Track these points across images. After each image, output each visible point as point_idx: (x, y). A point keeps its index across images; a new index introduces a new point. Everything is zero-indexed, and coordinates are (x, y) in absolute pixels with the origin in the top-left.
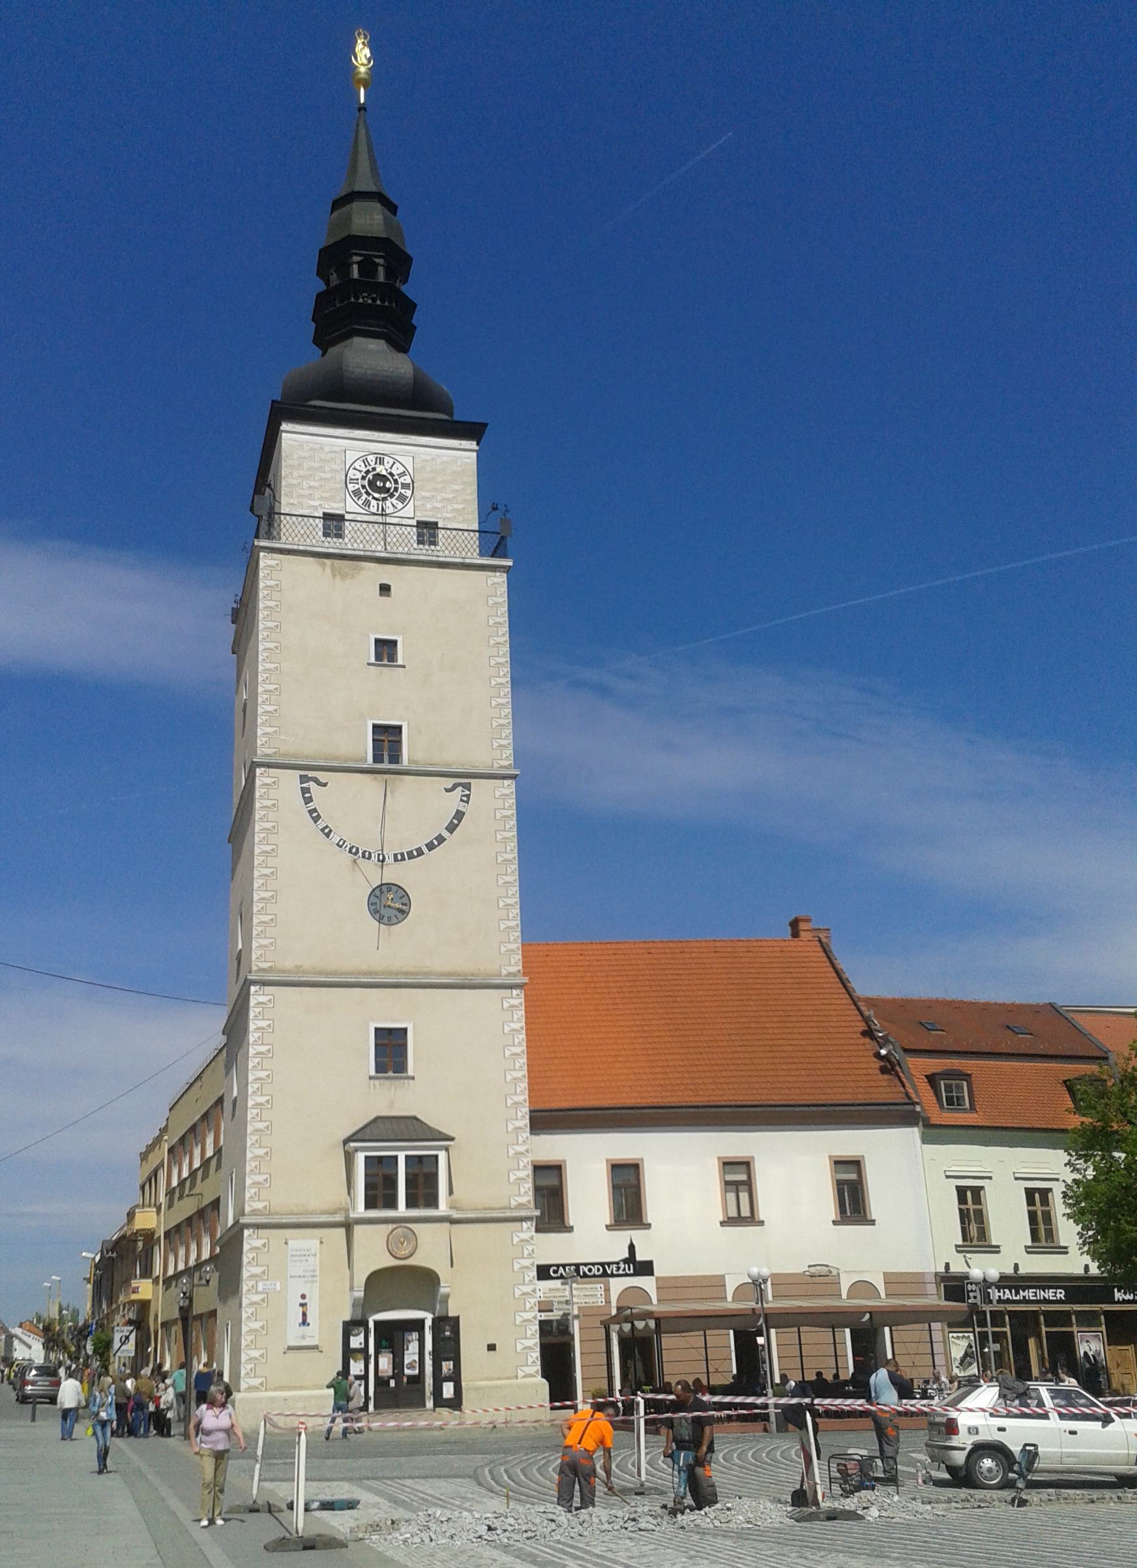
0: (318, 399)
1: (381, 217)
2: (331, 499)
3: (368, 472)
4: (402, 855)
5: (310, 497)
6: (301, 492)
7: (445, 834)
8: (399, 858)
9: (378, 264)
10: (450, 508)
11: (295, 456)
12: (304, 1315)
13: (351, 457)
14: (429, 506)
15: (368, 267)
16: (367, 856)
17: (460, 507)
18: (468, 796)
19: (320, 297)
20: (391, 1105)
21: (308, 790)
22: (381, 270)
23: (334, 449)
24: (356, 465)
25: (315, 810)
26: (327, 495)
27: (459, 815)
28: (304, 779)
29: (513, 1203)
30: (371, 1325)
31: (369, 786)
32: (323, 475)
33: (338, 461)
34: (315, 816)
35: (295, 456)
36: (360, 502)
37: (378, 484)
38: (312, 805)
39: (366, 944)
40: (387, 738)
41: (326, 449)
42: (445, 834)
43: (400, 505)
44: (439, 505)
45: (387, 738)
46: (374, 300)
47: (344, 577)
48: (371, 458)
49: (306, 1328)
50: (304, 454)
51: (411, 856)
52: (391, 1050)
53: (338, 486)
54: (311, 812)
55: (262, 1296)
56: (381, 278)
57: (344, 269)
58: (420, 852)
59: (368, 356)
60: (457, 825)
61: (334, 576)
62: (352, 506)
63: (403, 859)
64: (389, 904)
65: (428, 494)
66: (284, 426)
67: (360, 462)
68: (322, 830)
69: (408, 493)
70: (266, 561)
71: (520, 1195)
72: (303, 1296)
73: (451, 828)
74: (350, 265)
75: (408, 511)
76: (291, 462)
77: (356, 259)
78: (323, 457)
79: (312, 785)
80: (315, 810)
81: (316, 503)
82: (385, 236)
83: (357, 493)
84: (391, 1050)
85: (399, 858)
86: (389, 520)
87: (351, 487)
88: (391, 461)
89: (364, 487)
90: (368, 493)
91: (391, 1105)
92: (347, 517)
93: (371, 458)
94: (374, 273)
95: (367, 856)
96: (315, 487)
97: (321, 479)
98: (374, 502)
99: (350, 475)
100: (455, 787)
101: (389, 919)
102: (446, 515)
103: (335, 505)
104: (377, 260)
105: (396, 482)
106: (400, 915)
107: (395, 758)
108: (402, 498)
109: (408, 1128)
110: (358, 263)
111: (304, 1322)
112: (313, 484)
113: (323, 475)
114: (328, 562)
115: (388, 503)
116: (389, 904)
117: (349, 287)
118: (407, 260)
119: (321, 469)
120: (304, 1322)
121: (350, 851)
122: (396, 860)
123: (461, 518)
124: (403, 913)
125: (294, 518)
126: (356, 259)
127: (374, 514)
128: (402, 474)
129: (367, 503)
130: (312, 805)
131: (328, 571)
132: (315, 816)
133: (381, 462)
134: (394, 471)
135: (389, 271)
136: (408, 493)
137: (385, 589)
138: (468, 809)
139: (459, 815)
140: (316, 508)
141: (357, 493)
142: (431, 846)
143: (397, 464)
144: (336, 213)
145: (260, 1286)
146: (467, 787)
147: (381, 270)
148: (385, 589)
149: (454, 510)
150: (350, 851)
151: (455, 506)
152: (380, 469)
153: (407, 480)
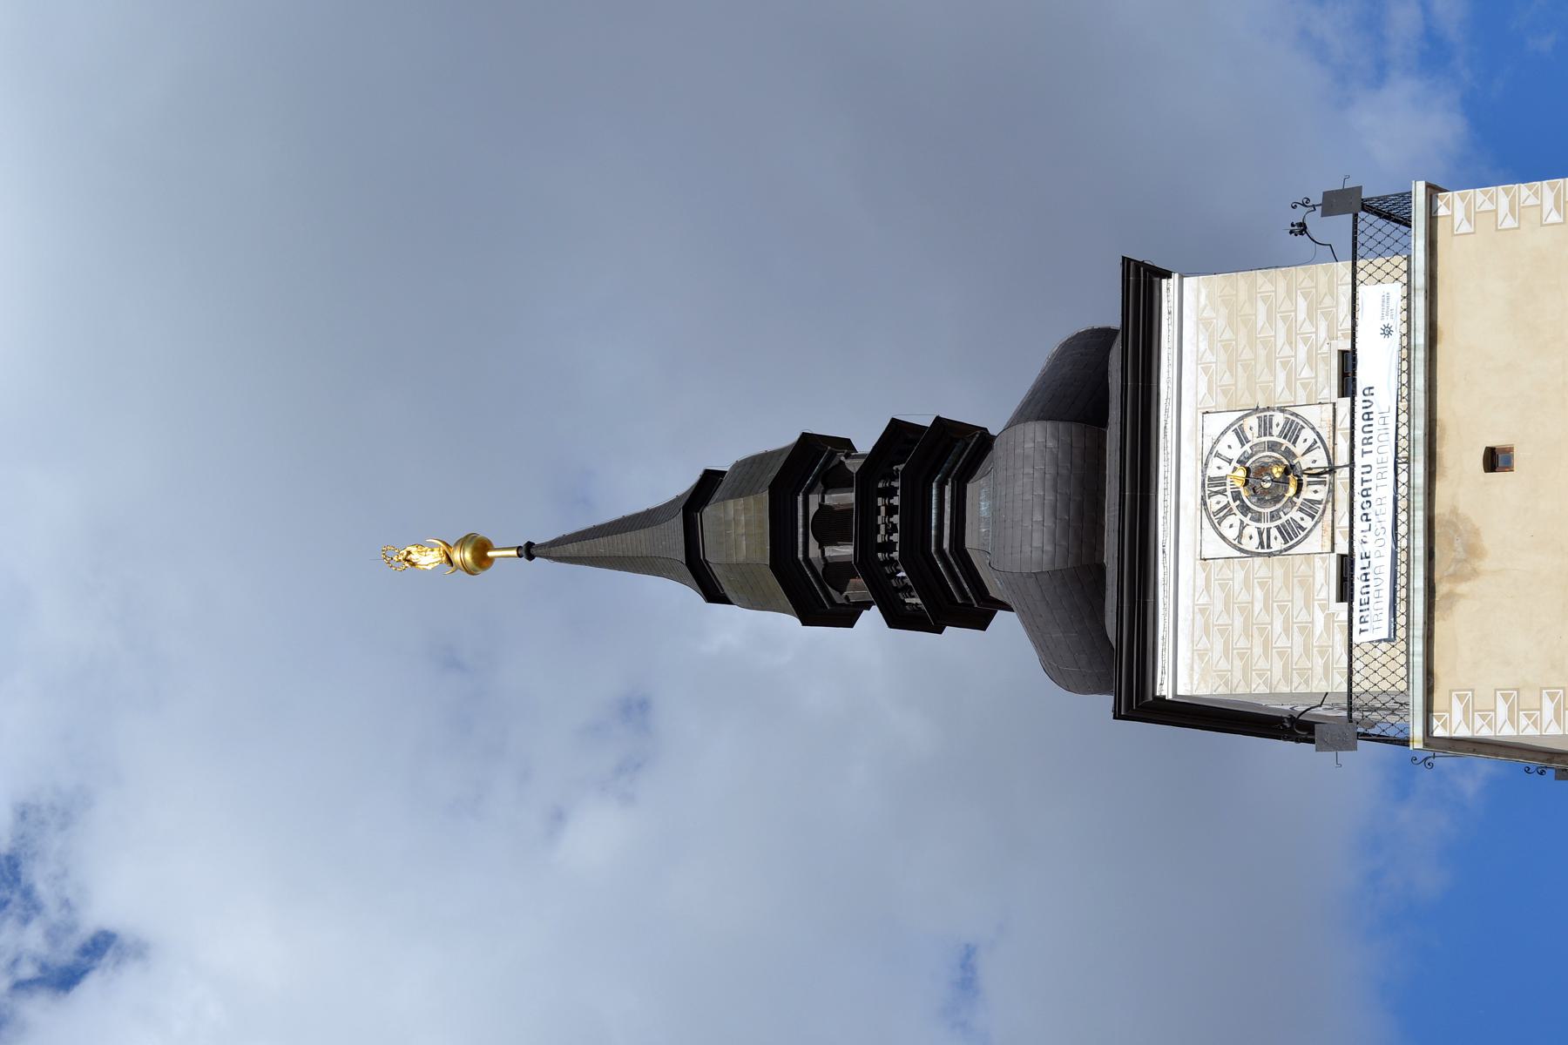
0: (1103, 627)
1: (731, 503)
2: (1307, 584)
3: (1245, 509)
6: (1298, 650)
9: (822, 506)
11: (1223, 665)
13: (1214, 547)
14: (1306, 373)
15: (829, 526)
17: (1302, 304)
19: (898, 618)
22: (832, 499)
23: (1201, 582)
24: (1231, 534)
26: (1299, 593)
32: (1258, 606)
33: (1227, 573)
35: (1223, 665)
36: (1308, 523)
37: (1271, 482)
41: (1203, 600)
43: (1308, 434)
44: (1302, 351)
46: (891, 510)
47: (1473, 551)
48: (1214, 503)
50: (1218, 646)
53: (1279, 572)
56: (848, 498)
57: (837, 573)
59: (1011, 518)
61: (1475, 573)
62: (1316, 542)
65: (1281, 377)
66: (1164, 690)
69: (1279, 418)
70: (1453, 723)
71: (1496, 211)
74: (828, 564)
75: (1318, 416)
76: (1238, 675)
77: (814, 551)
78: (1219, 606)
81: (1319, 617)
82: (766, 495)
83: (1288, 532)
86: (1342, 458)
87: (1277, 544)
88: (1215, 462)
92: (1343, 548)
93: (1214, 503)
94: (845, 513)
96: (1286, 620)
97: (1267, 607)
98: (1307, 493)
99: (1252, 545)
102: (1323, 334)
103: (1320, 576)
104: (813, 509)
108: (1291, 432)
110: (821, 547)
112: (1278, 627)
113: (1258, 606)
114: (1441, 589)
115: (1305, 462)
117: (868, 564)
118: (809, 445)
119: (1247, 611)
123: (1328, 301)
125: (1357, 665)
126: (814, 551)
127: (1332, 491)
129: (1310, 508)
131: (1462, 588)
133: (1221, 481)
134: (1236, 452)
135: (835, 479)
136: (1279, 418)
137: (1495, 460)
140: (1330, 617)
141: (1288, 532)
144: (730, 596)
147: (832, 499)
148: (1495, 460)
149: (1311, 315)
151: (1302, 315)
153: (1252, 421)
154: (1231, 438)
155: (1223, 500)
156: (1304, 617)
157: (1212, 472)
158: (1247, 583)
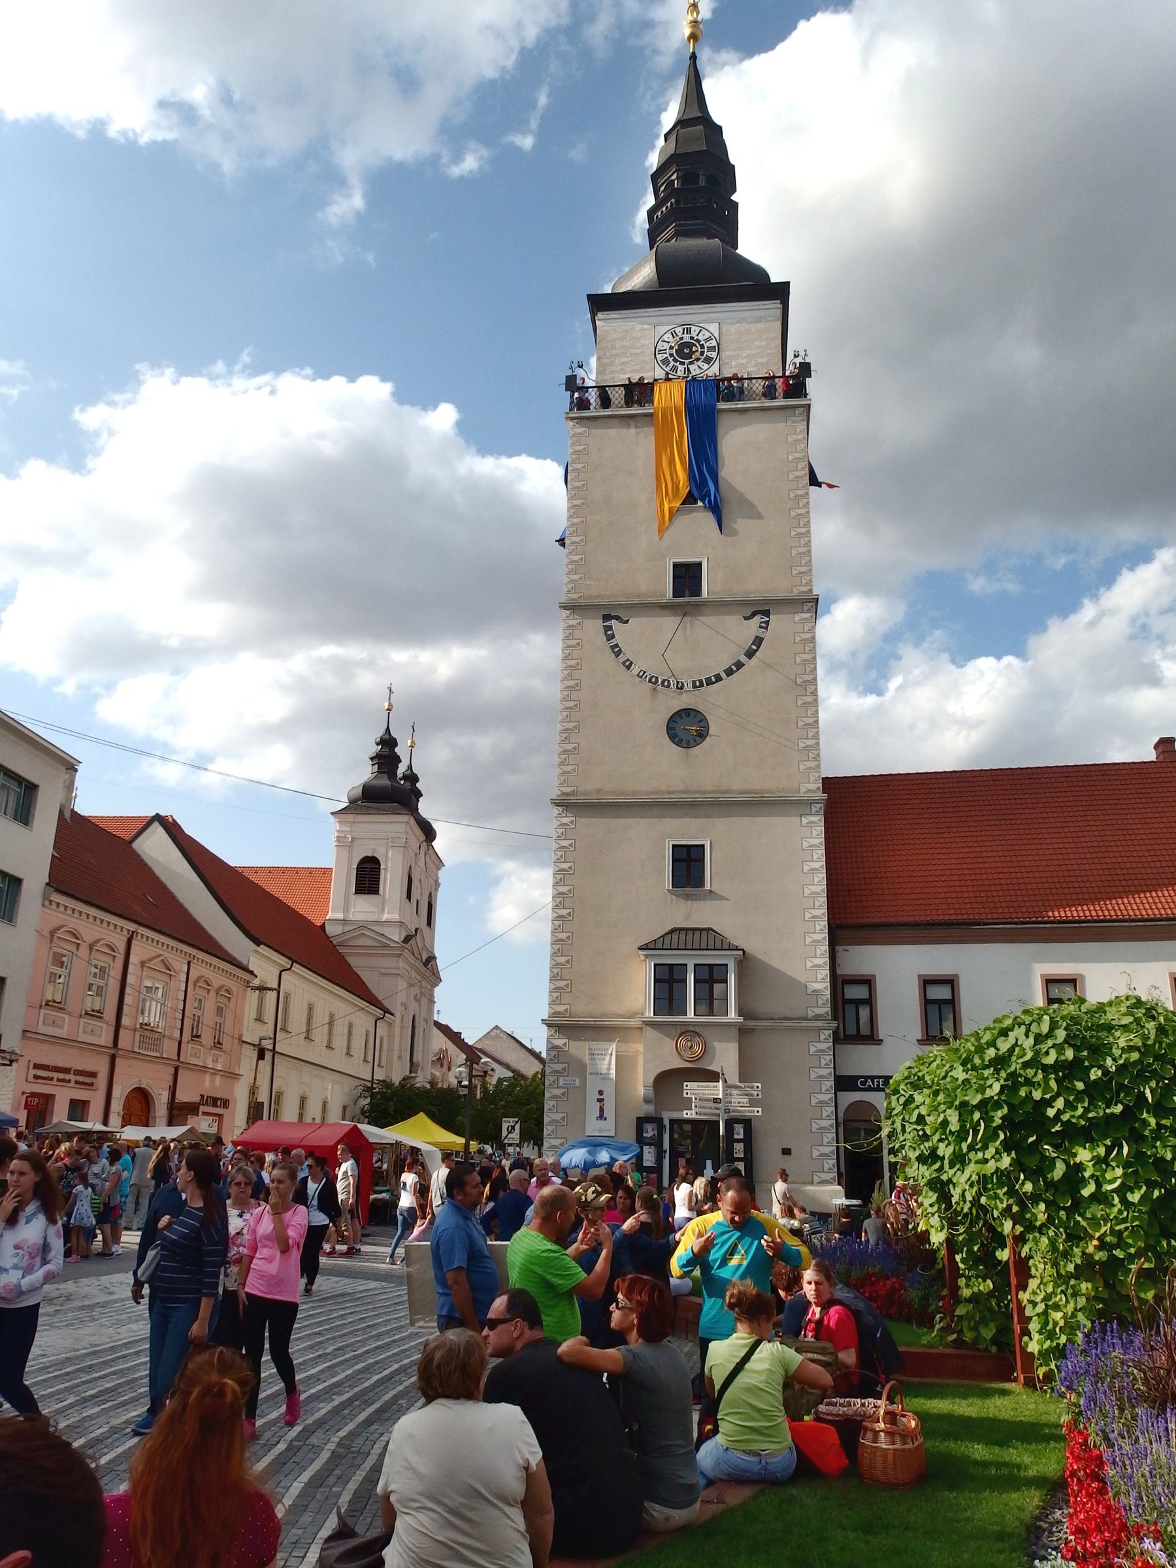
4: (701, 681)
5: (622, 371)
7: (743, 659)
8: (698, 685)
10: (754, 363)
12: (602, 1110)
16: (666, 684)
17: (764, 360)
18: (767, 623)
20: (687, 917)
21: (610, 628)
25: (617, 646)
27: (758, 641)
28: (607, 618)
29: (810, 1014)
30: (667, 1123)
31: (669, 622)
34: (617, 651)
38: (613, 642)
39: (666, 768)
40: (687, 577)
42: (743, 659)
43: (706, 366)
45: (687, 577)
49: (601, 1122)
51: (709, 682)
52: (688, 866)
54: (613, 647)
55: (562, 1091)
58: (718, 678)
60: (756, 651)
63: (701, 685)
64: (687, 728)
65: (733, 353)
67: (669, 335)
68: (624, 663)
69: (714, 355)
72: (601, 1093)
73: (750, 654)
79: (614, 623)
80: (617, 646)
83: (665, 362)
84: (688, 866)
85: (698, 685)
89: (671, 355)
90: (675, 360)
91: (687, 917)
95: (666, 684)
100: (754, 614)
101: (688, 742)
105: (702, 346)
106: (698, 739)
107: (697, 592)
108: (708, 360)
109: (705, 938)
111: (601, 1116)
116: (687, 728)
120: (601, 1116)
121: (650, 681)
122: (694, 686)
124: (702, 735)
128: (709, 339)
130: (613, 642)
132: (617, 651)
133: (689, 331)
134: (700, 337)
136: (714, 355)
138: (768, 635)
139: (758, 641)
142: (729, 672)
143: (704, 331)
145: (561, 1081)
146: (767, 613)
150: (650, 681)
151: (760, 360)
152: (687, 338)
153: (714, 343)
154: (708, 335)
155: (680, 335)
156: (628, 369)
157: (693, 328)
158: (642, 346)
